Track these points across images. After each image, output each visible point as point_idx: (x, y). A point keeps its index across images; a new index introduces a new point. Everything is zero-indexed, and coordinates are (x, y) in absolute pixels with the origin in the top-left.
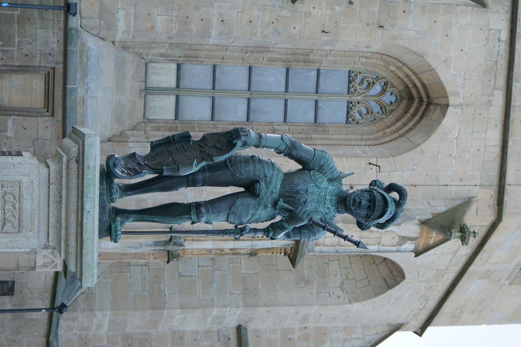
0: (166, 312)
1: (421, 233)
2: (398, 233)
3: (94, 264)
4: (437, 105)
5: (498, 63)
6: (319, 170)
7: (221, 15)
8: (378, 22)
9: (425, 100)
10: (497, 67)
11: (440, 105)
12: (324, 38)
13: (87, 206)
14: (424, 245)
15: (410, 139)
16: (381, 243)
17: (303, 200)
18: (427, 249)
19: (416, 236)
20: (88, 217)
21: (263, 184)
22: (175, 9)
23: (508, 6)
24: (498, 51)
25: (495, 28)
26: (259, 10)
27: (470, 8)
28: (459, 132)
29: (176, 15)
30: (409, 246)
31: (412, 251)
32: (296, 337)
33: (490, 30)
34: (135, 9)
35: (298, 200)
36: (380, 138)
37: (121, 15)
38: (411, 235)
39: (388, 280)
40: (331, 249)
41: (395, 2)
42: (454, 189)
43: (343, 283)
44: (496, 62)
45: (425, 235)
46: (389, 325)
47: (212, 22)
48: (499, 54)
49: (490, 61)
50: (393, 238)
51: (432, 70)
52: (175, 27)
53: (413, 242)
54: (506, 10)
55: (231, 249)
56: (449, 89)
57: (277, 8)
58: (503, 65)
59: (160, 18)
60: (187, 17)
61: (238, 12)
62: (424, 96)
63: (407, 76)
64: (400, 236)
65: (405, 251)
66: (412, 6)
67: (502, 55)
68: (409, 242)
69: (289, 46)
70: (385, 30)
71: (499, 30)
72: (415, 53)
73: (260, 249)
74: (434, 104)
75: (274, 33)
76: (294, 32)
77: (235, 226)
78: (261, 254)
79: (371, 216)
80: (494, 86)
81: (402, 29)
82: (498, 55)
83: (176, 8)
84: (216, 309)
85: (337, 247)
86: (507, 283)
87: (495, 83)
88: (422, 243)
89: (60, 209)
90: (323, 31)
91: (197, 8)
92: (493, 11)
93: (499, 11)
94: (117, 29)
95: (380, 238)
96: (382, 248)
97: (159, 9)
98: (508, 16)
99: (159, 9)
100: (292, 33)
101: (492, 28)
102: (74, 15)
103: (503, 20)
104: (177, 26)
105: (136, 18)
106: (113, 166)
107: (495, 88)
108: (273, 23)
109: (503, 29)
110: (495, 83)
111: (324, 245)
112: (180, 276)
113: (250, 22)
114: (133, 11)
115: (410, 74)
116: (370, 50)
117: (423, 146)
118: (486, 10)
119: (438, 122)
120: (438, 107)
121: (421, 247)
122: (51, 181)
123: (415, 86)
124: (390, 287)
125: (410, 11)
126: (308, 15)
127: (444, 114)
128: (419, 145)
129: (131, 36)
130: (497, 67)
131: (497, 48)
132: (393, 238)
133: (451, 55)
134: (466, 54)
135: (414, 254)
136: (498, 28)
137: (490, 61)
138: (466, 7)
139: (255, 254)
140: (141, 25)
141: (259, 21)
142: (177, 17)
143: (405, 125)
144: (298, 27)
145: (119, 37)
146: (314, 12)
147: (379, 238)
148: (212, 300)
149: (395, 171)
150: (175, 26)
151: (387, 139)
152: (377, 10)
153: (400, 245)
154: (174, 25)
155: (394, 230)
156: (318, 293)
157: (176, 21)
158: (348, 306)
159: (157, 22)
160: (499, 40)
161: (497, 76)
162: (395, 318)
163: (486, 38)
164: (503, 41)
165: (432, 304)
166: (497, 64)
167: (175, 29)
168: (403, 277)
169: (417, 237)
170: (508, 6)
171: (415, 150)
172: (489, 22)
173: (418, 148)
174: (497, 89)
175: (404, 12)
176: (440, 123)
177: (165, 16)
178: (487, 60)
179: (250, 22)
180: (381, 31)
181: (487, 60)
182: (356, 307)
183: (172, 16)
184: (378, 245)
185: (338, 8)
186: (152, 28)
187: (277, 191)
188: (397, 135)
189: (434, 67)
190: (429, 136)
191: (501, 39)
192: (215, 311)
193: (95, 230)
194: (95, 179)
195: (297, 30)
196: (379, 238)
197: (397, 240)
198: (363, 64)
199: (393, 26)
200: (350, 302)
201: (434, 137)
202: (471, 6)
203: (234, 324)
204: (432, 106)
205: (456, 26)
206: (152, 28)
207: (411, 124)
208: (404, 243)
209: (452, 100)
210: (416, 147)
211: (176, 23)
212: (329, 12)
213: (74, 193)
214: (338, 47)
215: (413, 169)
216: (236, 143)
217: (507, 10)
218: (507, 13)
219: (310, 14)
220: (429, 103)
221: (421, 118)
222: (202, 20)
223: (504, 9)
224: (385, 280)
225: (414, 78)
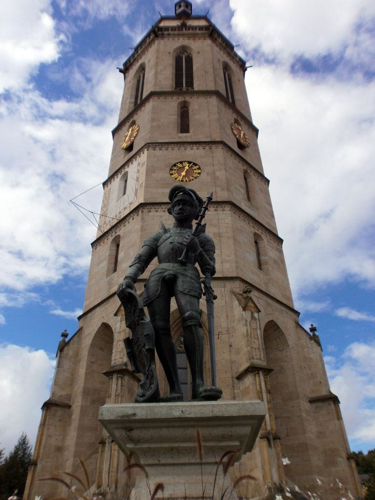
0: (308, 442)
1: (248, 310)
3: (240, 404)
6: (158, 242)
13: (177, 414)
17: (179, 245)
18: (256, 306)
20: (189, 413)
21: (166, 274)
30: (256, 315)
32: (310, 372)
35: (178, 247)
38: (250, 315)
39: (275, 328)
40: (262, 352)
42: (227, 299)
43: (280, 350)
46: (297, 328)
55: (268, 404)
69: (164, 382)
73: (266, 388)
77: (204, 295)
78: (269, 387)
79: (191, 203)
84: (303, 414)
85: (261, 349)
86: (269, 276)
88: (254, 310)
89: (186, 449)
95: (253, 329)
106: (144, 397)
111: (260, 355)
112: (287, 436)
115: (175, 324)
122: (157, 462)
124: (278, 327)
135: (260, 313)
139: (269, 391)
148: (298, 417)
149: (221, 325)
153: (256, 319)
156: (286, 362)
158: (291, 346)
162: (293, 324)
165: (284, 309)
168: (272, 321)
169: (251, 311)
182: (290, 343)
187: (172, 265)
192: (304, 415)
193: (202, 404)
194: (147, 407)
200: (288, 346)
203: (309, 404)
208: (255, 317)
213: (165, 432)
215: (219, 318)
216: (128, 292)
224: (275, 330)
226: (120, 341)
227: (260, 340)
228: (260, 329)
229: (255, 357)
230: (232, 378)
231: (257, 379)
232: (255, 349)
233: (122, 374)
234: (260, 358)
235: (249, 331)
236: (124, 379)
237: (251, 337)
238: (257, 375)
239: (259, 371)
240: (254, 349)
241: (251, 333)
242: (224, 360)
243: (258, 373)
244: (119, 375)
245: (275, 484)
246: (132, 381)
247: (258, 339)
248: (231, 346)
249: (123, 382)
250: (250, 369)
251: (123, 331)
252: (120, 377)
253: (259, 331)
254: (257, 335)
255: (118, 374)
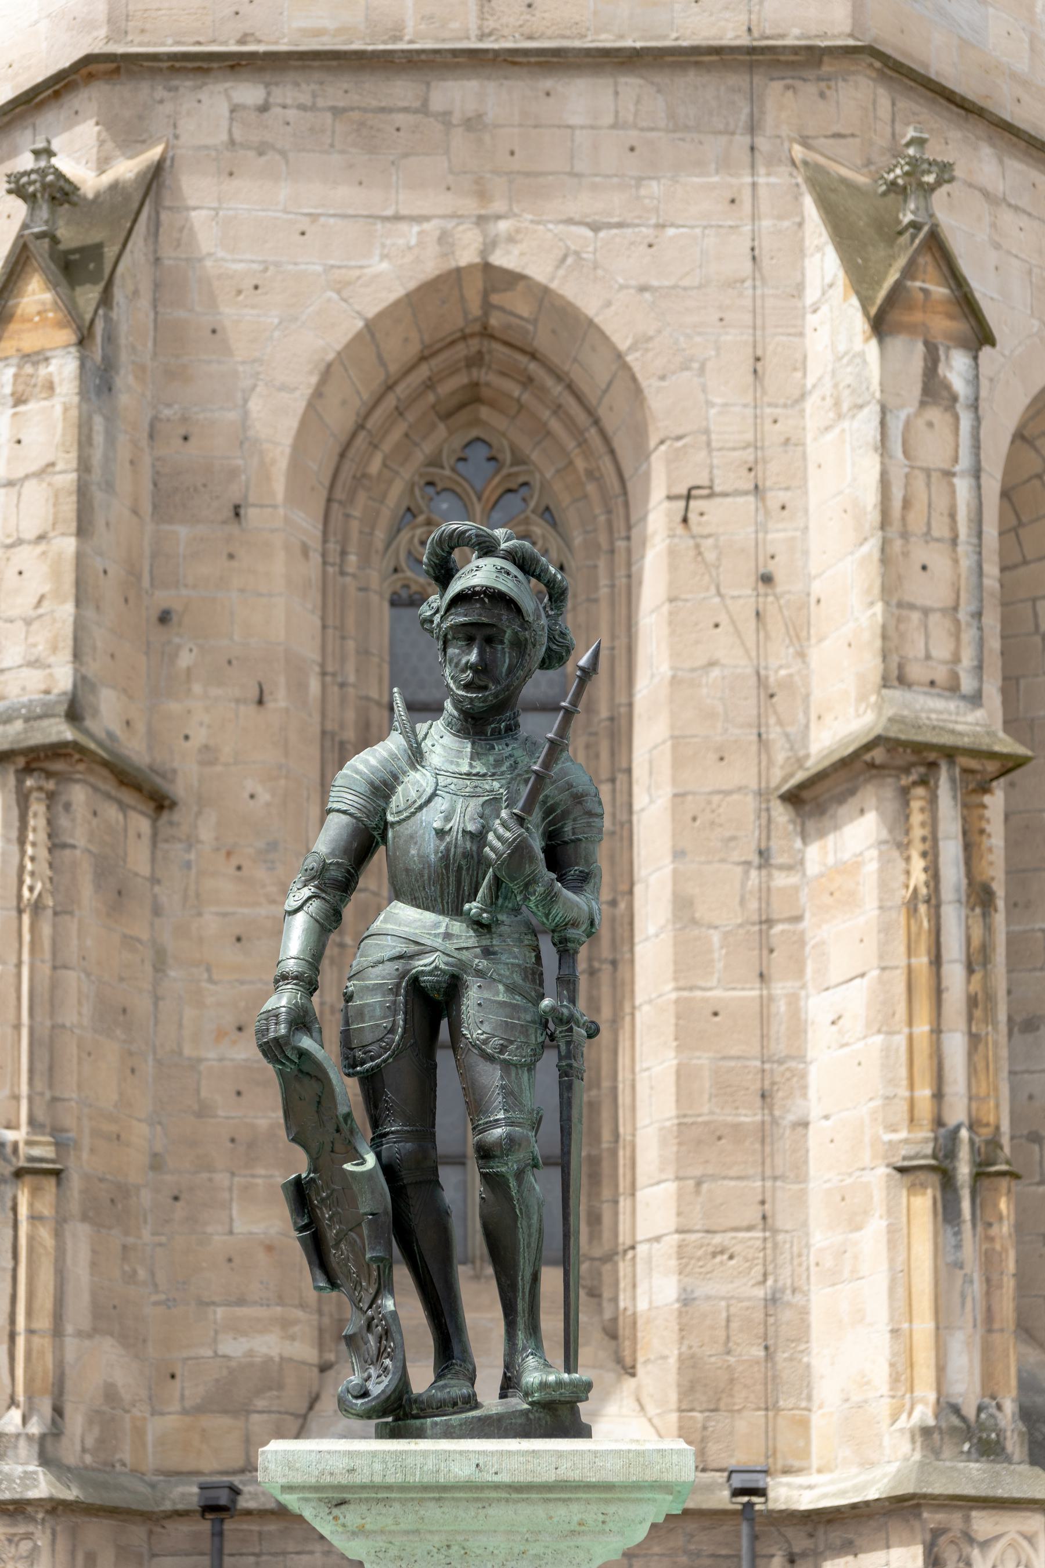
1: (911, 329)
2: (910, 410)
4: (487, 306)
5: (341, 104)
7: (220, 1035)
8: (224, 522)
9: (474, 344)
10: (352, 109)
11: (486, 294)
12: (280, 700)
14: (951, 317)
15: (603, 386)
16: (946, 466)
19: (920, 348)
22: (210, 1180)
23: (153, 88)
24: (302, 107)
25: (225, 124)
26: (200, 914)
27: (164, 216)
28: (570, 221)
29: (228, 1175)
31: (975, 358)
33: (232, 142)
34: (213, 1303)
36: (602, 489)
37: (234, 1347)
41: (158, 473)
44: (337, 112)
45: (918, 317)
47: (246, 1060)
48: (309, 104)
49: (333, 132)
50: (930, 425)
51: (371, 328)
52: (265, 1177)
53: (943, 357)
54: (166, 94)
55: (970, 970)
56: (430, 268)
57: (192, 856)
58: (345, 86)
59: (239, 1227)
60: (233, 1140)
61: (210, 980)
62: (461, 351)
63: (399, 412)
64: (923, 404)
65: (975, 381)
66: (167, 412)
67: (314, 96)
68: (942, 369)
70: (246, 497)
71: (232, 111)
72: (318, 393)
74: (486, 314)
75: (273, 862)
76: (264, 796)
80: (416, 111)
81: (242, 443)
82: (313, 108)
83: (205, 1175)
85: (963, 615)
87: (405, 110)
90: (260, 702)
91: (203, 1111)
92: (171, 137)
93: (169, 117)
94: (277, 1359)
95: (928, 472)
96: (965, 461)
97: (210, 1229)
98: (186, 84)
99: (210, 1229)
100: (268, 805)
101: (224, 137)
102: (235, 1491)
103: (199, 101)
104: (261, 1171)
105: (241, 1302)
107: (424, 109)
108: (239, 868)
109: (229, 98)
110: (405, 110)
111: (956, 659)
113: (239, 939)
114: (220, 1312)
115: (390, 401)
116: (316, 544)
117: (623, 344)
118: (168, 163)
119: (543, 295)
120: (495, 299)
121: (961, 326)
123: (430, 385)
125: (184, 419)
126: (208, 754)
127: (513, 279)
128: (619, 356)
129: (300, 1314)
130: (352, 109)
131: (291, 114)
132: (930, 425)
133: (319, 268)
134: (314, 217)
135: (986, 351)
136: (227, 114)
137: (333, 132)
138: (161, 230)
140: (262, 1283)
141: (233, 914)
142: (233, 1174)
143: (558, 409)
144: (251, 785)
145: (305, 1351)
146: (200, 736)
147: (929, 476)
149: (707, 432)
150: (260, 1176)
151: (606, 465)
152: (183, 532)
153: (954, 398)
154: (259, 1181)
155: (901, 425)
157: (245, 1176)
159: (251, 1233)
160: (264, 108)
161: (383, 104)
163: (261, 154)
164: (269, 94)
166: (344, 110)
167: (271, 1176)
169: (926, 343)
170: (153, 88)
171: (636, 368)
172: (206, 147)
173: (629, 359)
174: (425, 102)
175: (186, 438)
176: (546, 290)
177: (230, 1209)
178: (332, 146)
179: (239, 939)
180: (251, 514)
181: (332, 146)
183: (230, 1189)
184: (954, 474)
185: (185, 659)
186: (269, 1248)
188: (593, 433)
189: (360, 324)
190: (591, 323)
191: (260, 101)
195: (259, 789)
196: (929, 476)
197: (934, 414)
198: (365, 560)
199: (233, 474)
201: (589, 304)
202: (158, 213)
204: (495, 321)
205: (223, 259)
206: (269, 1248)
207: (557, 389)
209: (467, 256)
210: (626, 367)
211: (253, 1176)
212: (197, 688)
214: (311, 652)
215: (702, 370)
217: (165, 88)
218: (176, 89)
219: (206, 747)
220: (486, 333)
221: (533, 356)
222: (239, 1093)
223: (161, 102)
225: (402, 390)
226: (19, 542)
227: (961, 549)
228: (977, 473)
229: (916, 672)
230: (762, 794)
231: (917, 818)
232: (926, 612)
233: (49, 775)
234: (955, 677)
235: (897, 494)
236: (67, 806)
237: (905, 535)
238: (920, 791)
239: (933, 765)
240: (916, 616)
241: (906, 504)
242: (715, 673)
243: (923, 782)
244: (29, 783)
245: (956, 1410)
246: (112, 812)
247: (954, 541)
248: (767, 579)
249: (64, 821)
250: (878, 755)
251: (40, 474)
252: (40, 789)
253: (963, 486)
254: (952, 516)
255: (28, 770)
